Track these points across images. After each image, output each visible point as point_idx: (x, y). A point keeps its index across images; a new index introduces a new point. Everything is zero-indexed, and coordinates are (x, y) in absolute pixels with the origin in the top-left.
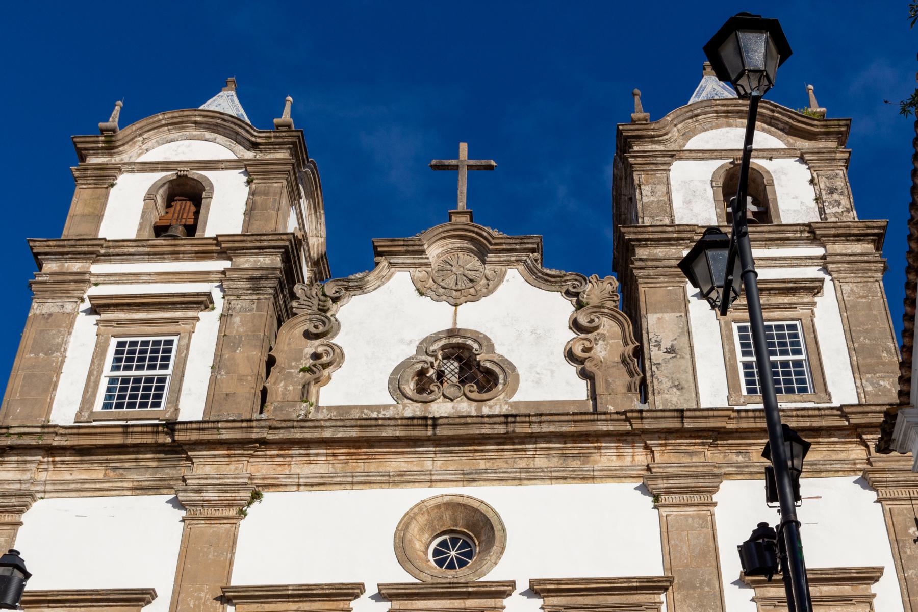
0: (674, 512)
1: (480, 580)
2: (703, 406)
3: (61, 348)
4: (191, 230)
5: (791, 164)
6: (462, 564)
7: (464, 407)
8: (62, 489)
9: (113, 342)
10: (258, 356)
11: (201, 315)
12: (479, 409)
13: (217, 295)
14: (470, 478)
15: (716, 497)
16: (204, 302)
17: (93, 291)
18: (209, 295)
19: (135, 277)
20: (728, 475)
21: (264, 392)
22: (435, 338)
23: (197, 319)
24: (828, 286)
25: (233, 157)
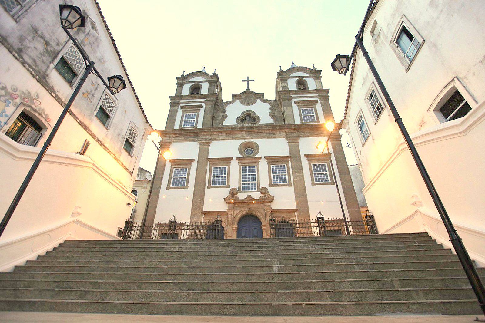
0: (291, 144)
1: (256, 156)
2: (296, 124)
3: (176, 116)
4: (198, 94)
5: (311, 79)
6: (251, 154)
7: (250, 125)
8: (177, 141)
9: (185, 114)
10: (211, 116)
11: (201, 109)
12: (253, 125)
13: (204, 106)
14: (252, 138)
15: (299, 141)
16: (201, 106)
17: (181, 105)
18: (202, 105)
19: (188, 102)
20: (301, 137)
21: (213, 123)
22: (244, 112)
23: (200, 110)
24: (319, 101)
25: (205, 80)
